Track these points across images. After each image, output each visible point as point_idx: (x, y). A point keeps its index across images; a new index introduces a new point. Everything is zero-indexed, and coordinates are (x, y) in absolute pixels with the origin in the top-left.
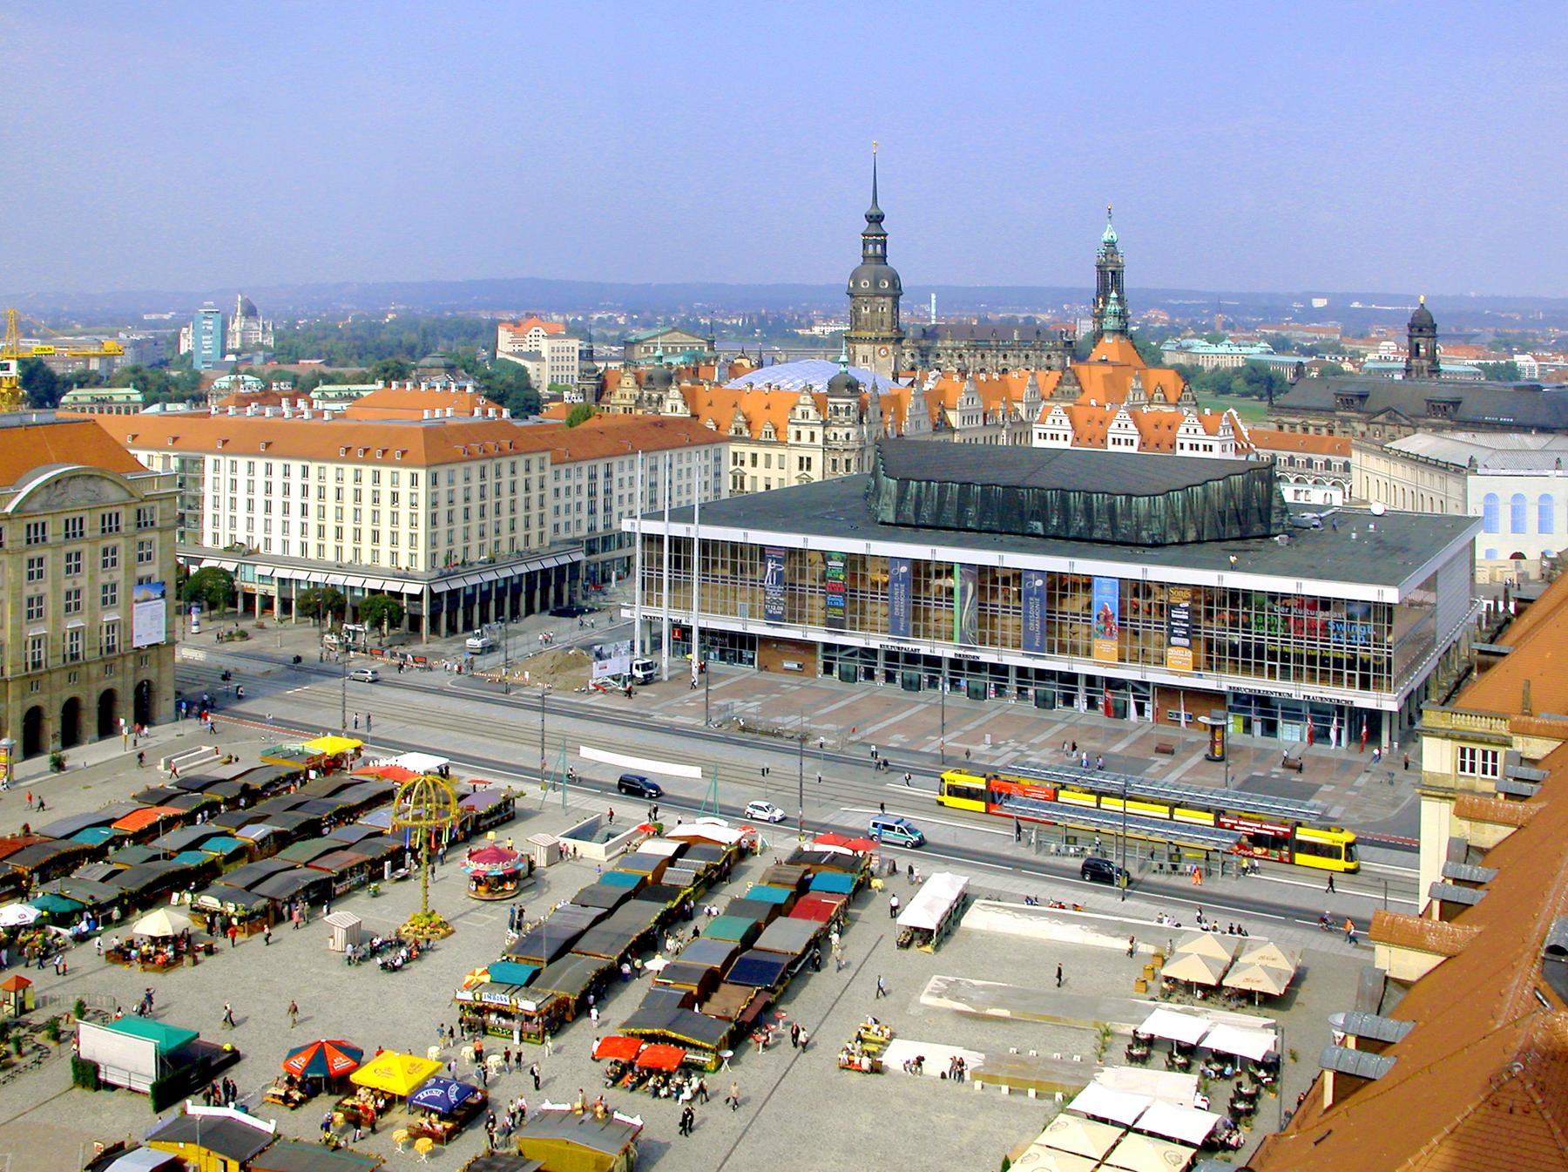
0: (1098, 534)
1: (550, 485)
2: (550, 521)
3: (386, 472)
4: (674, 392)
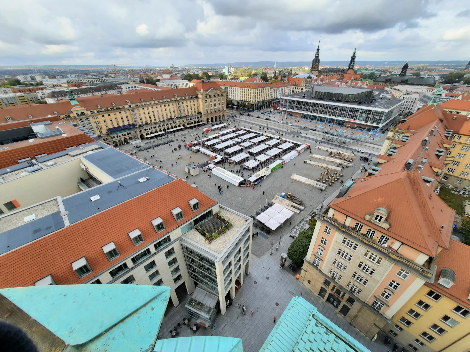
0: (343, 100)
1: (270, 91)
2: (269, 96)
3: (250, 89)
4: (286, 78)
